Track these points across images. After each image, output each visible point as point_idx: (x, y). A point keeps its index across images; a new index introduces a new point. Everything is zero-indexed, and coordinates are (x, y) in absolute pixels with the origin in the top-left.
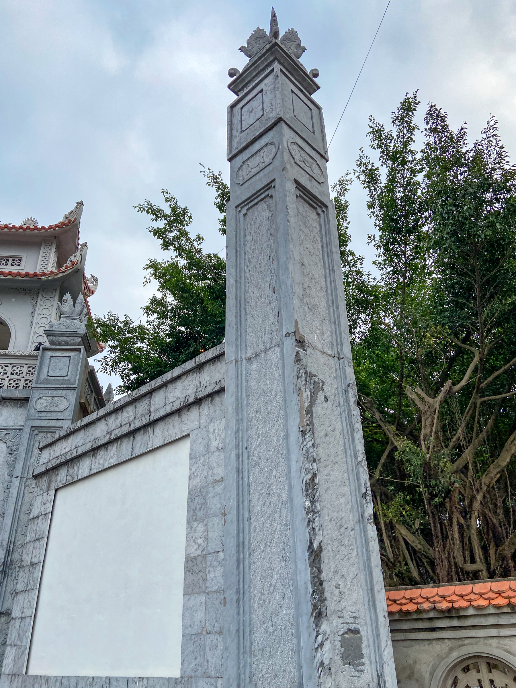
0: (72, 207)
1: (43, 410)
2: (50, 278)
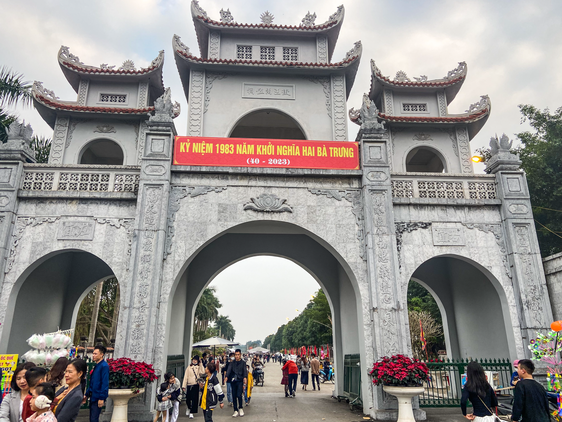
0: (457, 66)
1: (515, 212)
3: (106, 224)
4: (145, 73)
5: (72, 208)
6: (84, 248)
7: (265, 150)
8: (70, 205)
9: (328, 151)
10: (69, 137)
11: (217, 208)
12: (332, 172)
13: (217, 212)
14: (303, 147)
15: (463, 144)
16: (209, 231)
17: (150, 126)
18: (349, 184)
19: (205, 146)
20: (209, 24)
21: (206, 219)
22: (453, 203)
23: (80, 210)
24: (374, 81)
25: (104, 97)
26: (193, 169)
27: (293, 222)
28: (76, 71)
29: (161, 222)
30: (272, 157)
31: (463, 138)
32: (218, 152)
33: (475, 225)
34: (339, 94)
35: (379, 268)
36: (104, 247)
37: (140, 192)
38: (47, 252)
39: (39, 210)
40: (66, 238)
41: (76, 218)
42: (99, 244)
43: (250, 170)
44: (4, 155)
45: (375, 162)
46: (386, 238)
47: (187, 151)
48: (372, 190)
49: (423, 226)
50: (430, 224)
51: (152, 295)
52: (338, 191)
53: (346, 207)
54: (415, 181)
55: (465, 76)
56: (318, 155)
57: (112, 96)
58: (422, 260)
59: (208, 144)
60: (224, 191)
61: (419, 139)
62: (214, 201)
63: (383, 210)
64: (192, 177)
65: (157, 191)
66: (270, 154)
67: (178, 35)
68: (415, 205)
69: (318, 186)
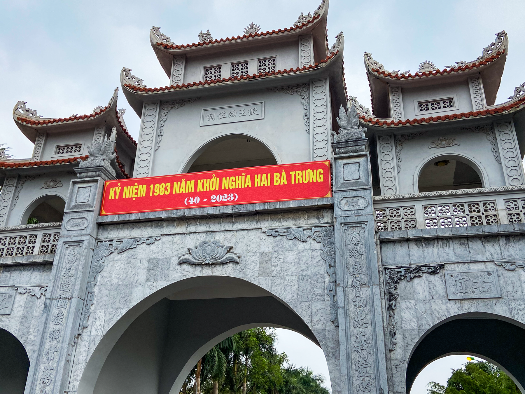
0: (493, 39)
2: (511, 112)
3: (26, 294)
4: (97, 116)
7: (208, 185)
9: (289, 177)
10: (15, 198)
11: (146, 265)
12: (292, 204)
13: (146, 270)
14: (256, 176)
15: (507, 146)
16: (134, 295)
17: (80, 173)
18: (318, 218)
19: (137, 189)
20: (169, 50)
21: (132, 280)
22: (476, 233)
24: (371, 79)
26: (122, 218)
27: (240, 276)
28: (29, 125)
29: (76, 287)
30: (216, 192)
31: (506, 137)
32: (151, 195)
33: (517, 264)
34: (318, 103)
35: (354, 337)
36: (21, 322)
37: (58, 252)
42: (17, 319)
43: (187, 213)
45: (351, 185)
46: (365, 292)
47: (117, 198)
48: (345, 224)
49: (430, 270)
50: (442, 267)
51: (55, 382)
52: (302, 229)
53: (313, 250)
54: (419, 206)
55: (504, 50)
56: (275, 184)
57: (68, 147)
58: (430, 322)
59: (140, 186)
60: (156, 243)
61: (439, 147)
62: (144, 256)
63: (363, 250)
64: (122, 229)
65: (77, 248)
66: (212, 189)
67: (128, 67)
68: (418, 241)
69: (276, 224)
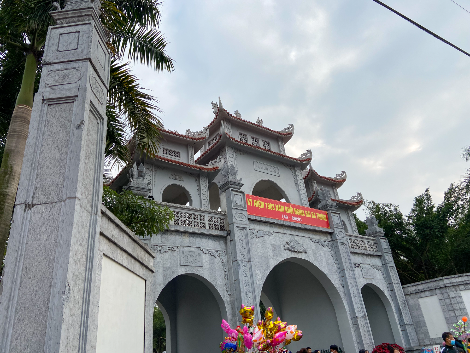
5: (186, 240)
6: (198, 273)
8: (184, 238)
16: (270, 263)
23: (191, 241)
25: (165, 150)
36: (210, 273)
38: (175, 276)
39: (164, 240)
40: (186, 264)
41: (189, 248)
44: (136, 192)
65: (243, 232)
